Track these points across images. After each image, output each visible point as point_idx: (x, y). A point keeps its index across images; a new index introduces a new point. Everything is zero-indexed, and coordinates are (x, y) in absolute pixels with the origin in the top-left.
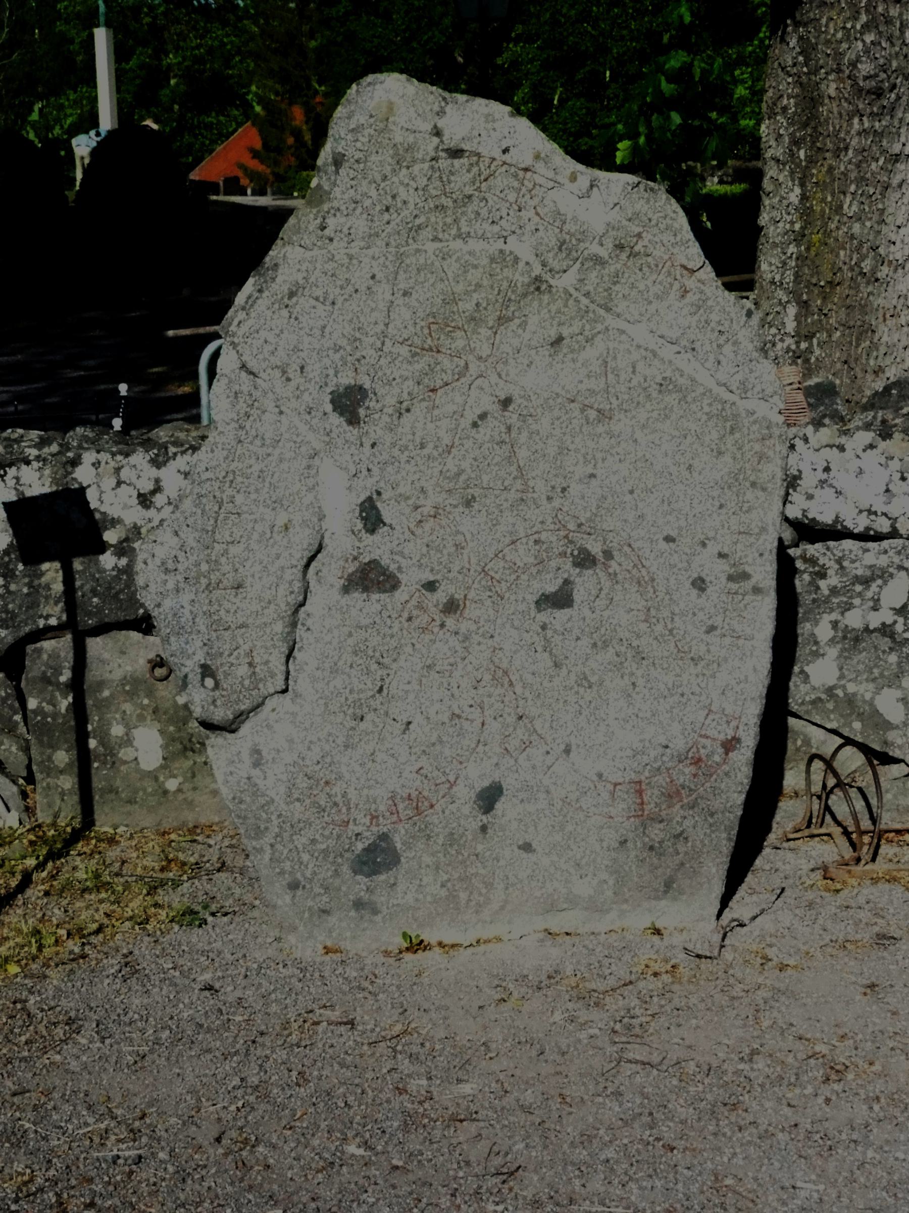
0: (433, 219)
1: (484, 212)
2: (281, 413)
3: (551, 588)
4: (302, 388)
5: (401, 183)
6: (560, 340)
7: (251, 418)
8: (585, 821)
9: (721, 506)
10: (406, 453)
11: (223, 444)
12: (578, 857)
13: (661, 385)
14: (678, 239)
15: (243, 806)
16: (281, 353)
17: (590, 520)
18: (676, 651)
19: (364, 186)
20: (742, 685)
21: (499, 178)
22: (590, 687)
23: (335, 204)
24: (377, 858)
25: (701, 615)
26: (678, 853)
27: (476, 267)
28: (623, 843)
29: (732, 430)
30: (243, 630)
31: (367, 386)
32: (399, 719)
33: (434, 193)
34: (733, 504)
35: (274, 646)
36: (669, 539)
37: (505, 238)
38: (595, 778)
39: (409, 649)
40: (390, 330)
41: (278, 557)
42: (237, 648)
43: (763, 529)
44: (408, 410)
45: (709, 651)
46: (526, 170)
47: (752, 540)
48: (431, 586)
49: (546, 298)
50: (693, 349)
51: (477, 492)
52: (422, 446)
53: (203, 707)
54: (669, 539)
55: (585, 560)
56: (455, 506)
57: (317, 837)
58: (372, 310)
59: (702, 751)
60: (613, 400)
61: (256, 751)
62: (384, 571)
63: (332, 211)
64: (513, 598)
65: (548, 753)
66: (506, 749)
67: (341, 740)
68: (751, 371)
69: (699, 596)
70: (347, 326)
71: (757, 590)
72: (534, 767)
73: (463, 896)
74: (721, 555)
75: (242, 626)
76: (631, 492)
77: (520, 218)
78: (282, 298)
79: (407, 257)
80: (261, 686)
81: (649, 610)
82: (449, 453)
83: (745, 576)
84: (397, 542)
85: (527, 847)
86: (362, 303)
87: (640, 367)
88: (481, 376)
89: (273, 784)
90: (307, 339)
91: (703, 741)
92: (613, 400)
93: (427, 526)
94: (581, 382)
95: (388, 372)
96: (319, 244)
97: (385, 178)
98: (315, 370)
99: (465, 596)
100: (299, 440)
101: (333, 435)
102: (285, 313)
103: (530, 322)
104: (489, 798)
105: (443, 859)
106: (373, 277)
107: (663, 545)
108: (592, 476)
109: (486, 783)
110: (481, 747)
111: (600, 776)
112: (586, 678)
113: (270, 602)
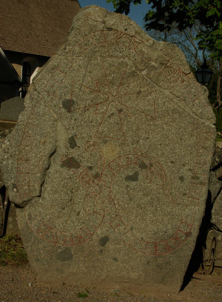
0: (101, 50)
1: (118, 49)
2: (46, 106)
3: (131, 174)
4: (53, 99)
5: (91, 37)
6: (140, 92)
7: (36, 107)
8: (136, 254)
9: (191, 153)
10: (86, 124)
11: (27, 114)
12: (133, 265)
13: (173, 110)
14: (182, 63)
15: (24, 232)
16: (48, 87)
17: (145, 152)
18: (172, 200)
19: (79, 37)
20: (194, 215)
21: (123, 39)
22: (141, 209)
23: (69, 42)
24: (66, 256)
25: (181, 189)
26: (167, 269)
27: (113, 66)
28: (148, 262)
29: (196, 129)
30: (27, 174)
31: (75, 100)
32: (76, 210)
33: (102, 41)
34: (195, 153)
35: (37, 181)
36: (172, 162)
37: (124, 57)
38: (140, 239)
39: (81, 188)
40: (84, 83)
41: (41, 152)
42: (25, 180)
43: (205, 163)
44: (88, 110)
45: (183, 202)
46: (132, 37)
47: (201, 166)
48: (91, 168)
49: (136, 78)
50: (185, 100)
51: (108, 139)
52: (92, 122)
53: (12, 197)
54: (172, 162)
55: (143, 166)
56: (101, 143)
57: (46, 245)
58: (79, 76)
59: (178, 235)
60: (157, 114)
61: (30, 215)
62: (76, 161)
63: (68, 44)
64: (118, 176)
65: (125, 229)
66: (111, 225)
67: (56, 215)
68: (204, 109)
69: (181, 183)
70: (70, 81)
71: (202, 183)
72: (120, 233)
73: (93, 272)
74: (190, 170)
75: (28, 173)
76: (160, 145)
77: (129, 52)
78: (50, 70)
79: (91, 60)
80: (31, 193)
81: (164, 185)
82: (100, 125)
83: (198, 178)
84: (80, 152)
85: (116, 259)
86: (75, 74)
87: (166, 104)
88: (113, 101)
89: (33, 225)
90: (56, 83)
91: (179, 232)
92: (157, 114)
93: (91, 148)
94: (146, 107)
95: (82, 97)
96: (63, 54)
97: (86, 35)
98: (58, 93)
99: (102, 173)
100: (51, 115)
101: (62, 115)
102: (50, 75)
103: (131, 85)
104: (104, 241)
105: (87, 259)
106: (80, 66)
107: (170, 164)
108: (148, 138)
109: (103, 236)
110: (102, 224)
111: (142, 239)
112: (140, 205)
113: (37, 166)
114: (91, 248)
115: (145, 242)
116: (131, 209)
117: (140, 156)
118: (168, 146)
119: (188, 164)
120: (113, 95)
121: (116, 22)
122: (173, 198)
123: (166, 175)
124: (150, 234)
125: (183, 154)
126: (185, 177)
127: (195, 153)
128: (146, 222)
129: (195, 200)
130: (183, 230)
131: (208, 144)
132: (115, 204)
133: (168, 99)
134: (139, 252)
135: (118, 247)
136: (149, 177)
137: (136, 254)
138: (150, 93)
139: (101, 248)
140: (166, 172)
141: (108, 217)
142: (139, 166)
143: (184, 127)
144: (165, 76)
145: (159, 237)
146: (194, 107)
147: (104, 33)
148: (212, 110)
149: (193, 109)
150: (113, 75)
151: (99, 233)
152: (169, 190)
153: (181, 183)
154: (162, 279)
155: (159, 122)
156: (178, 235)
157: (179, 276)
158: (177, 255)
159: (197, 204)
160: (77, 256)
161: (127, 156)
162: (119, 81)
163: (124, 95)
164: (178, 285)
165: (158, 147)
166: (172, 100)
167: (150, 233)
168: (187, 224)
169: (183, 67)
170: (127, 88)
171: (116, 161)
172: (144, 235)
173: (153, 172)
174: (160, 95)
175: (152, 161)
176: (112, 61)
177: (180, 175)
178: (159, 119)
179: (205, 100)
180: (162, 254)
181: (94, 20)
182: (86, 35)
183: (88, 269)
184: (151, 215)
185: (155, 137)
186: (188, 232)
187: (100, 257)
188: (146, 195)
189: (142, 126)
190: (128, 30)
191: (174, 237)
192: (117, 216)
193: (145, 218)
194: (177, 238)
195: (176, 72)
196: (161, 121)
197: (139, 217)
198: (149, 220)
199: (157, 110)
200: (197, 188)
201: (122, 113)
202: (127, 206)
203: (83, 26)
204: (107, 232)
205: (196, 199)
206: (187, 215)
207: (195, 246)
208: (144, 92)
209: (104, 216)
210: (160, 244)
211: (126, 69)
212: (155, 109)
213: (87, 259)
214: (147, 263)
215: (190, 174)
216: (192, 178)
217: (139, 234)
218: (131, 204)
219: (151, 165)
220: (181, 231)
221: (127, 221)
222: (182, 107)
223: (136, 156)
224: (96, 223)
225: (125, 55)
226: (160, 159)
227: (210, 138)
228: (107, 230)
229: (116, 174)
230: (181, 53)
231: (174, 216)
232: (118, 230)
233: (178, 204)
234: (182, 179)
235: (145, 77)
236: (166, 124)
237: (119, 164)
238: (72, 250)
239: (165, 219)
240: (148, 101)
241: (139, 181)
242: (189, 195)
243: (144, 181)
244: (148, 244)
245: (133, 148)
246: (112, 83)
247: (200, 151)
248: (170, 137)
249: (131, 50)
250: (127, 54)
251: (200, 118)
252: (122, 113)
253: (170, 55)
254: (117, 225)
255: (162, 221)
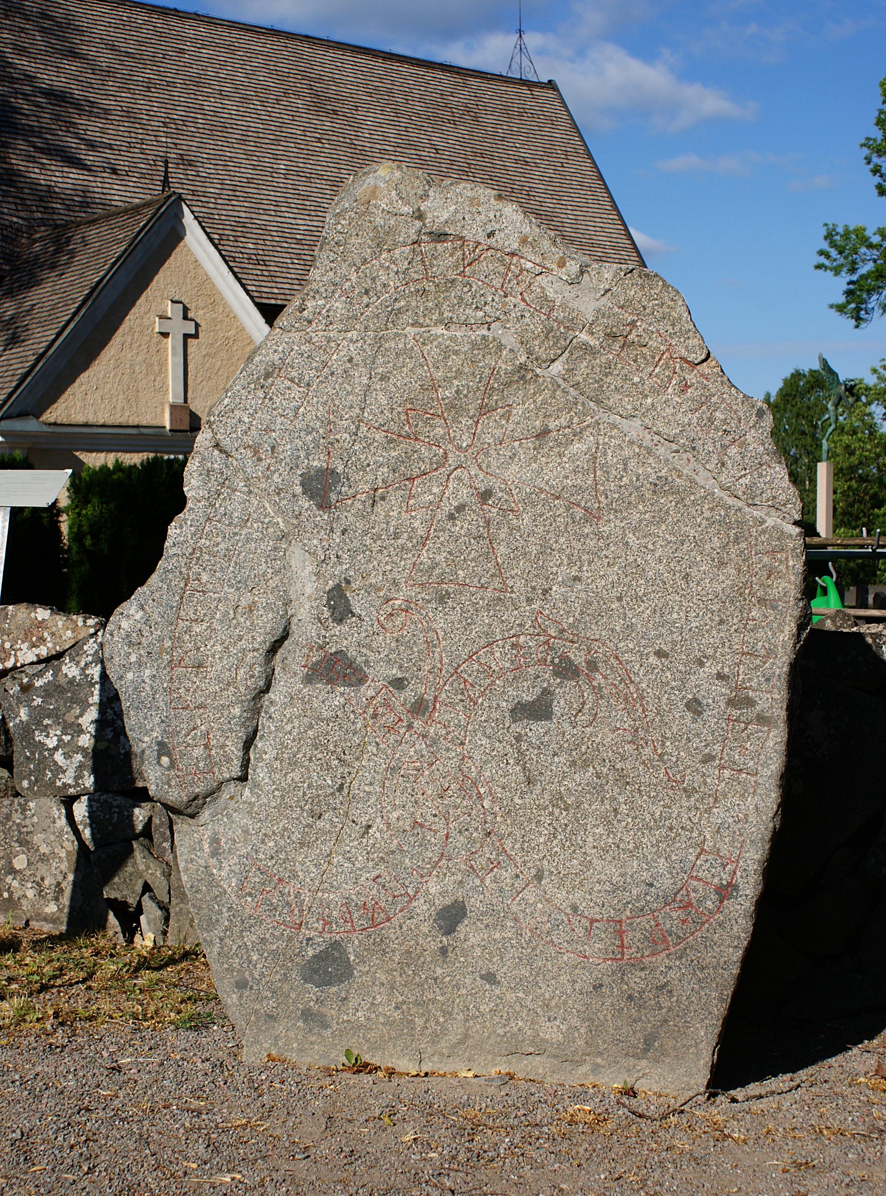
0: (414, 304)
1: (468, 298)
2: (250, 492)
3: (528, 698)
4: (272, 468)
5: (382, 266)
6: (544, 433)
7: (222, 497)
8: (556, 958)
9: (721, 622)
10: (379, 543)
11: (192, 521)
12: (547, 996)
13: (656, 485)
14: (677, 328)
15: (199, 896)
16: (254, 432)
17: (571, 626)
18: (666, 779)
19: (344, 269)
20: (739, 826)
21: (484, 264)
22: (566, 809)
23: (314, 286)
24: (328, 967)
25: (696, 743)
26: (660, 1008)
27: (456, 353)
28: (598, 987)
29: (737, 541)
30: (201, 711)
31: (340, 469)
32: (359, 821)
33: (416, 277)
34: (735, 621)
35: (231, 730)
36: (660, 654)
37: (489, 324)
38: (569, 911)
39: (372, 748)
40: (366, 414)
41: (240, 638)
42: (194, 729)
43: (770, 653)
44: (383, 498)
45: (705, 783)
46: (513, 254)
47: (758, 662)
48: (399, 684)
49: (532, 388)
50: (694, 449)
51: (452, 588)
52: (396, 536)
53: (157, 786)
54: (660, 654)
55: (566, 670)
56: (429, 602)
57: (267, 936)
58: (348, 394)
59: (693, 895)
60: (602, 499)
61: (215, 841)
62: (351, 664)
63: (312, 294)
64: (486, 704)
65: (517, 876)
66: (472, 867)
67: (296, 836)
68: (761, 476)
69: (694, 721)
70: (321, 408)
71: (761, 719)
72: (501, 890)
73: (419, 1022)
74: (720, 676)
75: (201, 706)
76: (620, 599)
77: (505, 304)
78: (258, 379)
79: (387, 341)
80: (216, 770)
81: (636, 731)
82: (424, 545)
83: (750, 703)
84: (364, 635)
85: (490, 978)
86: (337, 386)
87: (632, 464)
88: (460, 466)
89: (226, 873)
90: (279, 420)
91: (695, 883)
92: (602, 499)
93: (398, 621)
94: (567, 477)
95: (363, 457)
96: (297, 325)
97: (365, 261)
98: (286, 449)
99: (436, 697)
100: (266, 520)
101: (302, 518)
102: (260, 394)
103: (514, 412)
104: (451, 917)
105: (399, 979)
106: (350, 360)
107: (653, 660)
108: (576, 579)
109: (448, 901)
110: (444, 861)
111: (575, 908)
112: (561, 798)
113: (229, 684)
114: (411, 943)
115: (583, 920)
116: (534, 811)
117: (555, 638)
118: (643, 601)
119: (714, 657)
120: (459, 448)
121: (456, 211)
122: (669, 771)
123: (642, 698)
124: (600, 891)
125: (694, 625)
126: (705, 702)
127: (735, 621)
128: (585, 853)
129: (744, 775)
130: (709, 876)
131: (778, 588)
132: (480, 797)
133: (637, 450)
134: (568, 951)
135: (497, 936)
136: (588, 706)
137: (556, 958)
138: (578, 434)
139: (441, 942)
140: (644, 686)
141: (462, 838)
142: (553, 670)
143: (694, 537)
144: (626, 375)
145: (628, 903)
146: (724, 469)
147: (421, 251)
148: (787, 477)
149: (722, 478)
150: (456, 383)
151: (432, 891)
152: (655, 746)
153: (694, 721)
154: (645, 1041)
155: (610, 526)
156: (693, 895)
157: (703, 1033)
158: (692, 961)
159: (751, 790)
160: (367, 968)
161: (514, 639)
162: (478, 399)
163: (495, 445)
164: (702, 1062)
165: (613, 606)
166: (650, 452)
167: (597, 887)
168: (720, 857)
169: (682, 340)
170: (504, 422)
171: (478, 658)
172: (578, 895)
173: (600, 688)
174: (611, 437)
175: (596, 652)
176: (450, 339)
177: (690, 697)
178: (612, 517)
179: (763, 444)
180: (642, 956)
181: (389, 212)
182: (365, 261)
183: (403, 1012)
184: (598, 831)
185: (602, 573)
186: (725, 883)
187: (439, 971)
188: (580, 763)
189: (556, 542)
190: (499, 236)
191: (681, 901)
192: (490, 833)
193: (579, 838)
194: (690, 904)
195: (660, 360)
196: (618, 523)
197: (559, 837)
198: (594, 847)
199: (602, 488)
200: (748, 737)
201: (490, 502)
202: (519, 802)
203: (355, 233)
204: (458, 889)
205: (747, 774)
206: (719, 828)
207: (751, 929)
208: (559, 430)
209: (447, 838)
210: (635, 924)
211: (496, 362)
212: (596, 484)
213: (399, 979)
214: (594, 987)
215: (723, 690)
216: (730, 703)
217: (564, 893)
218: (532, 793)
219: (592, 666)
220: (700, 880)
221: (523, 849)
222: (685, 472)
223: (542, 638)
224: (423, 860)
225: (493, 314)
226: (621, 645)
227: (782, 568)
228: (460, 882)
229: (480, 700)
230: (671, 295)
231: (675, 831)
232: (495, 881)
233: (688, 792)
234: (695, 707)
235: (560, 381)
236: (635, 530)
237: (491, 668)
238: (351, 950)
239: (645, 840)
240: (573, 459)
241: (555, 721)
242: (721, 759)
243: (573, 718)
244: (595, 924)
245: (532, 611)
246: (455, 407)
247: (753, 614)
248: (650, 573)
249: (510, 298)
250: (498, 313)
251: (749, 505)
252: (490, 502)
253: (638, 306)
254: (491, 866)
255: (637, 847)
